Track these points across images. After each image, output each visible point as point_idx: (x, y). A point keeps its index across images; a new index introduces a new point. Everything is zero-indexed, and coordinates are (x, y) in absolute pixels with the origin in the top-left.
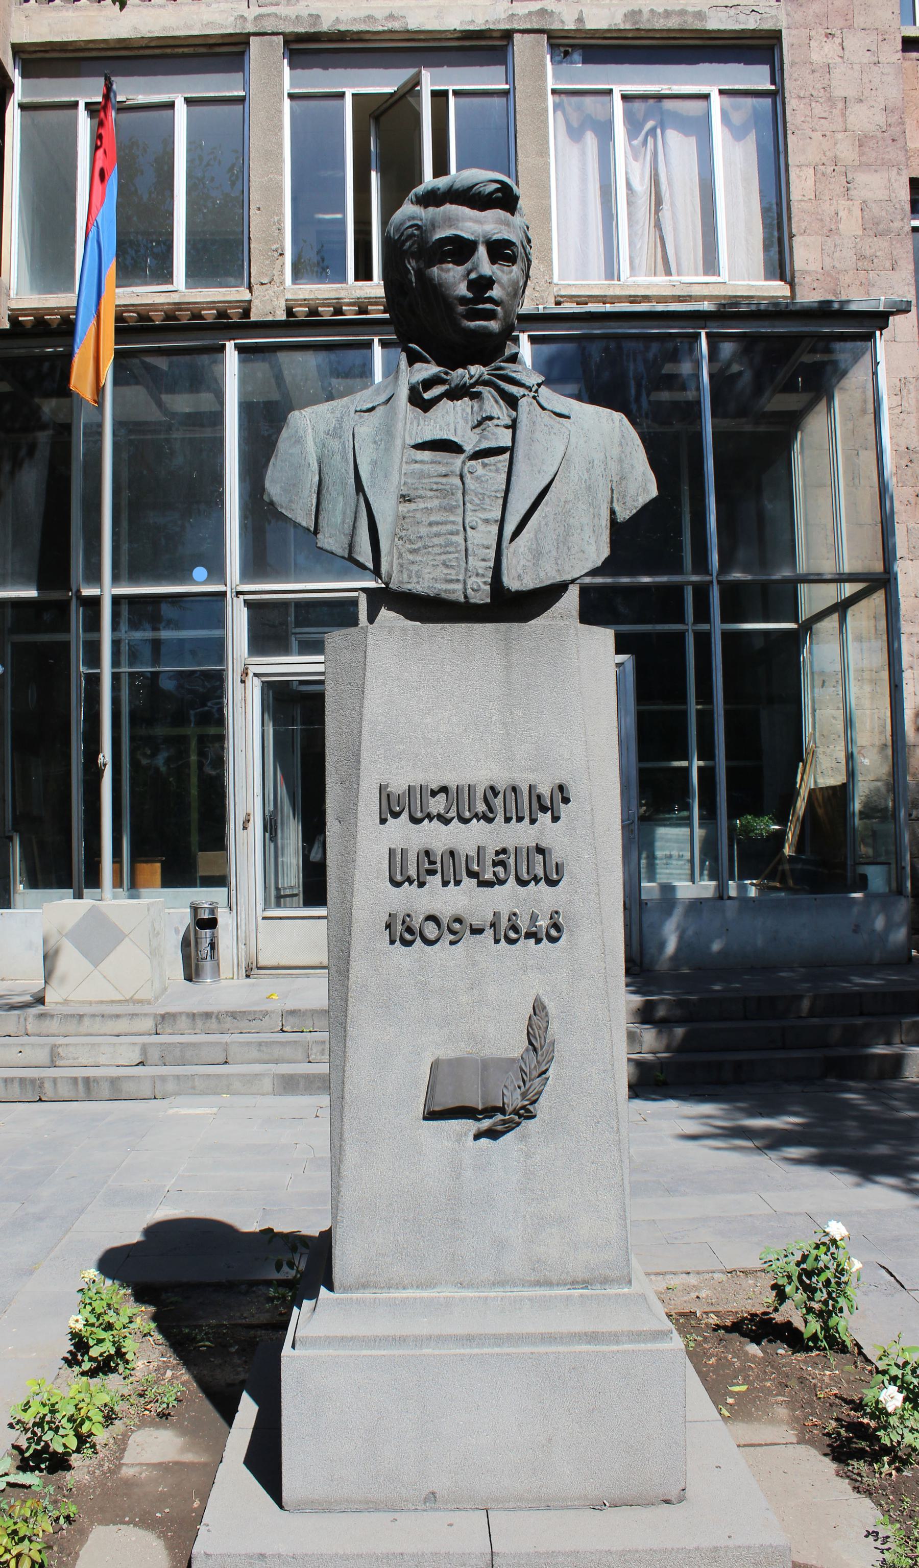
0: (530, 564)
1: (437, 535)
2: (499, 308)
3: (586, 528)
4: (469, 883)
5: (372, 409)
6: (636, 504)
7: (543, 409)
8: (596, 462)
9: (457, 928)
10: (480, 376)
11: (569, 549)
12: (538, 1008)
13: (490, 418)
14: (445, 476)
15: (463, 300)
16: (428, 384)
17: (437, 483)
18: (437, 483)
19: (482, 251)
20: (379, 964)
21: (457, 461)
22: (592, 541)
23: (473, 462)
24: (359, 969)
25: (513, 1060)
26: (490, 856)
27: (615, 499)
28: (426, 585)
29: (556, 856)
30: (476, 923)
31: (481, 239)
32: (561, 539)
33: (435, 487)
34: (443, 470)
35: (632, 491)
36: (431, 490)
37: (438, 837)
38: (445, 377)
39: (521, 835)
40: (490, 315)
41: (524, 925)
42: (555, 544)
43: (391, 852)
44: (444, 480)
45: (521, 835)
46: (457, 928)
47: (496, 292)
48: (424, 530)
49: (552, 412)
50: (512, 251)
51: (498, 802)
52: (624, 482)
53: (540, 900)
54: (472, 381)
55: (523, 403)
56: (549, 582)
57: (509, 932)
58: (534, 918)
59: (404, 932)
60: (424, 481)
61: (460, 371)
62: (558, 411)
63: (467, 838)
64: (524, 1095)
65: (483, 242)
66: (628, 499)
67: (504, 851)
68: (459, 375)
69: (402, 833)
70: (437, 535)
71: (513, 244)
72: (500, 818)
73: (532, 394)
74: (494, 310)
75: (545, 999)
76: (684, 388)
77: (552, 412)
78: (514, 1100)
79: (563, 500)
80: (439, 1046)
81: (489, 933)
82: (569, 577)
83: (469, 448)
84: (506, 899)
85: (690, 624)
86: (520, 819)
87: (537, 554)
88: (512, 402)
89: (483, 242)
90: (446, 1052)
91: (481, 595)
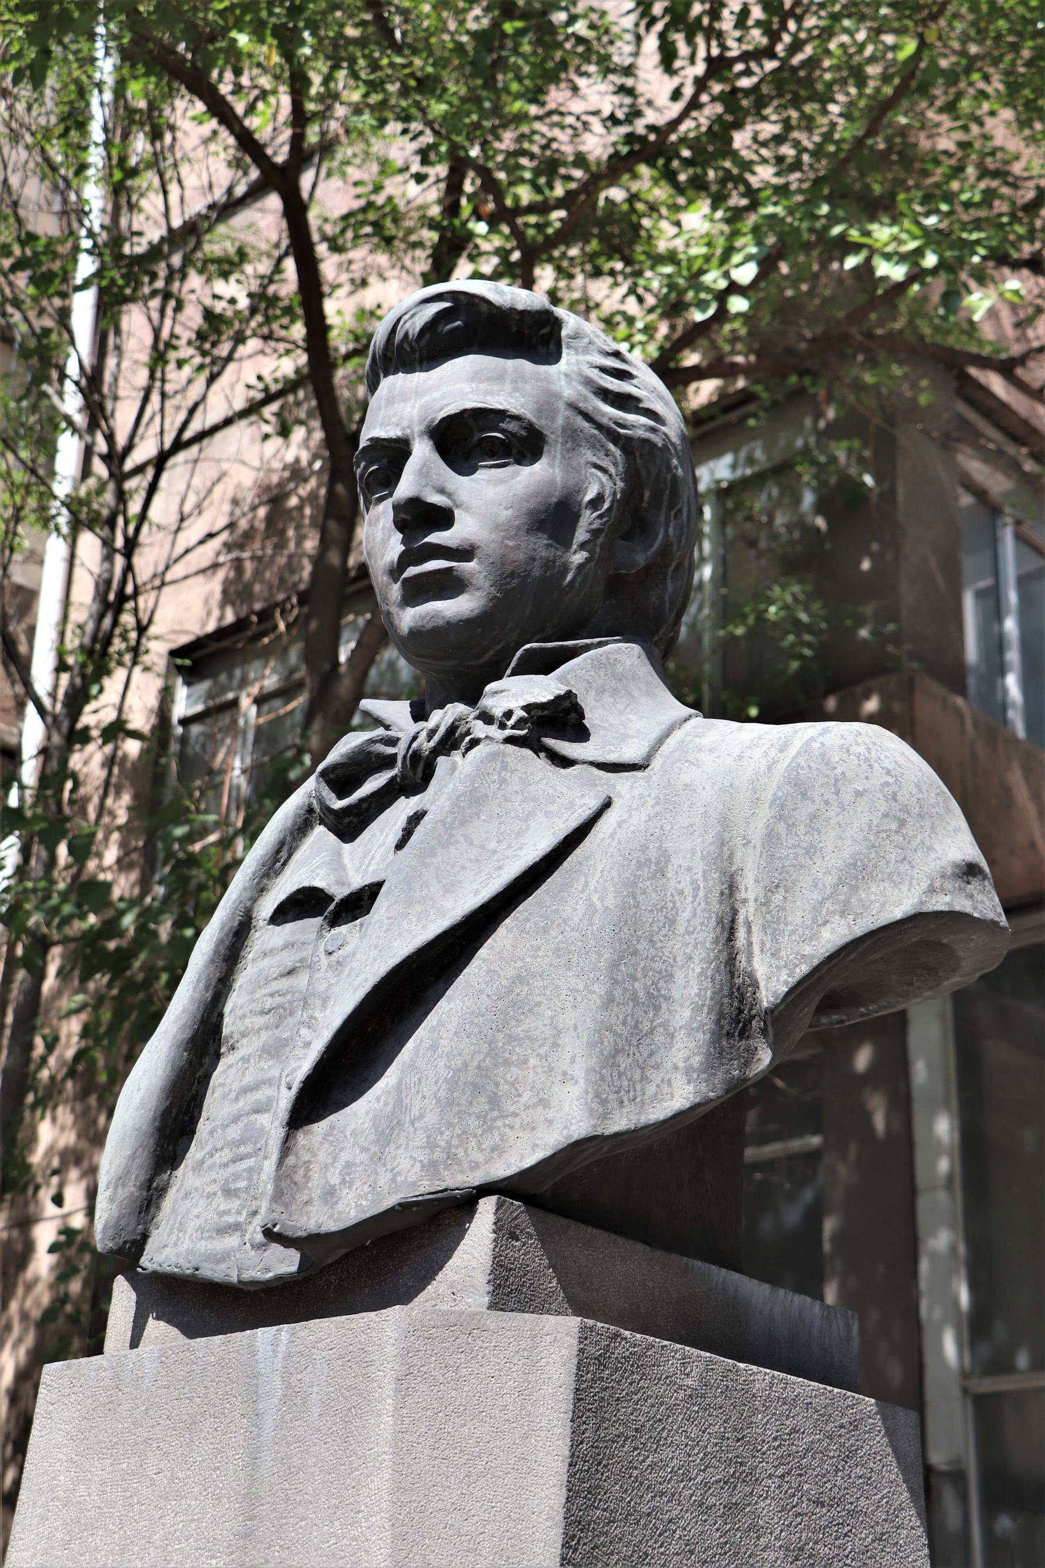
0: (364, 1157)
2: (472, 564)
3: (566, 1039)
6: (807, 950)
8: (676, 861)
10: (452, 729)
11: (494, 1102)
14: (290, 972)
17: (272, 995)
18: (272, 995)
22: (578, 1071)
23: (343, 929)
27: (756, 948)
28: (186, 1245)
31: (418, 428)
32: (471, 1075)
33: (269, 1003)
35: (798, 915)
36: (263, 1013)
38: (390, 750)
40: (447, 585)
42: (442, 1094)
44: (285, 984)
47: (463, 530)
49: (592, 763)
50: (503, 431)
52: (777, 898)
54: (432, 744)
56: (390, 1201)
60: (257, 995)
62: (612, 757)
65: (422, 434)
66: (784, 940)
70: (236, 1119)
71: (502, 414)
73: (508, 732)
74: (451, 569)
77: (592, 763)
79: (510, 972)
82: (476, 1178)
87: (388, 1129)
89: (422, 434)
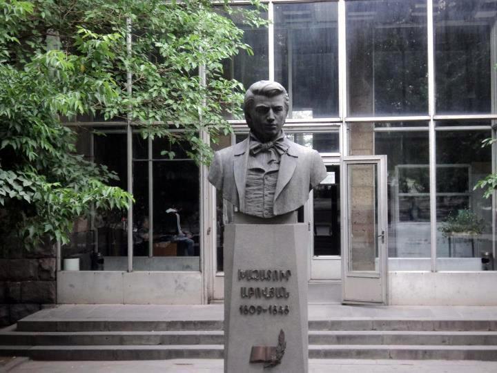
1: (256, 197)
4: (262, 298)
5: (239, 155)
7: (289, 155)
9: (259, 310)
12: (282, 333)
13: (273, 160)
15: (266, 125)
16: (255, 149)
19: (271, 111)
20: (239, 320)
21: (262, 175)
24: (232, 321)
25: (274, 348)
26: (269, 290)
29: (287, 290)
30: (265, 308)
34: (258, 177)
37: (254, 285)
39: (278, 285)
41: (277, 309)
43: (242, 288)
45: (278, 285)
46: (259, 310)
48: (252, 196)
51: (271, 276)
53: (281, 303)
55: (283, 156)
57: (274, 311)
58: (281, 307)
59: (244, 311)
61: (265, 144)
63: (262, 285)
64: (277, 357)
67: (273, 288)
68: (265, 145)
69: (245, 284)
72: (272, 280)
75: (284, 330)
76: (419, 23)
78: (274, 358)
80: (252, 343)
81: (268, 312)
83: (266, 171)
84: (274, 302)
85: (432, 121)
86: (277, 279)
88: (280, 155)
90: (255, 345)
91: (266, 214)
